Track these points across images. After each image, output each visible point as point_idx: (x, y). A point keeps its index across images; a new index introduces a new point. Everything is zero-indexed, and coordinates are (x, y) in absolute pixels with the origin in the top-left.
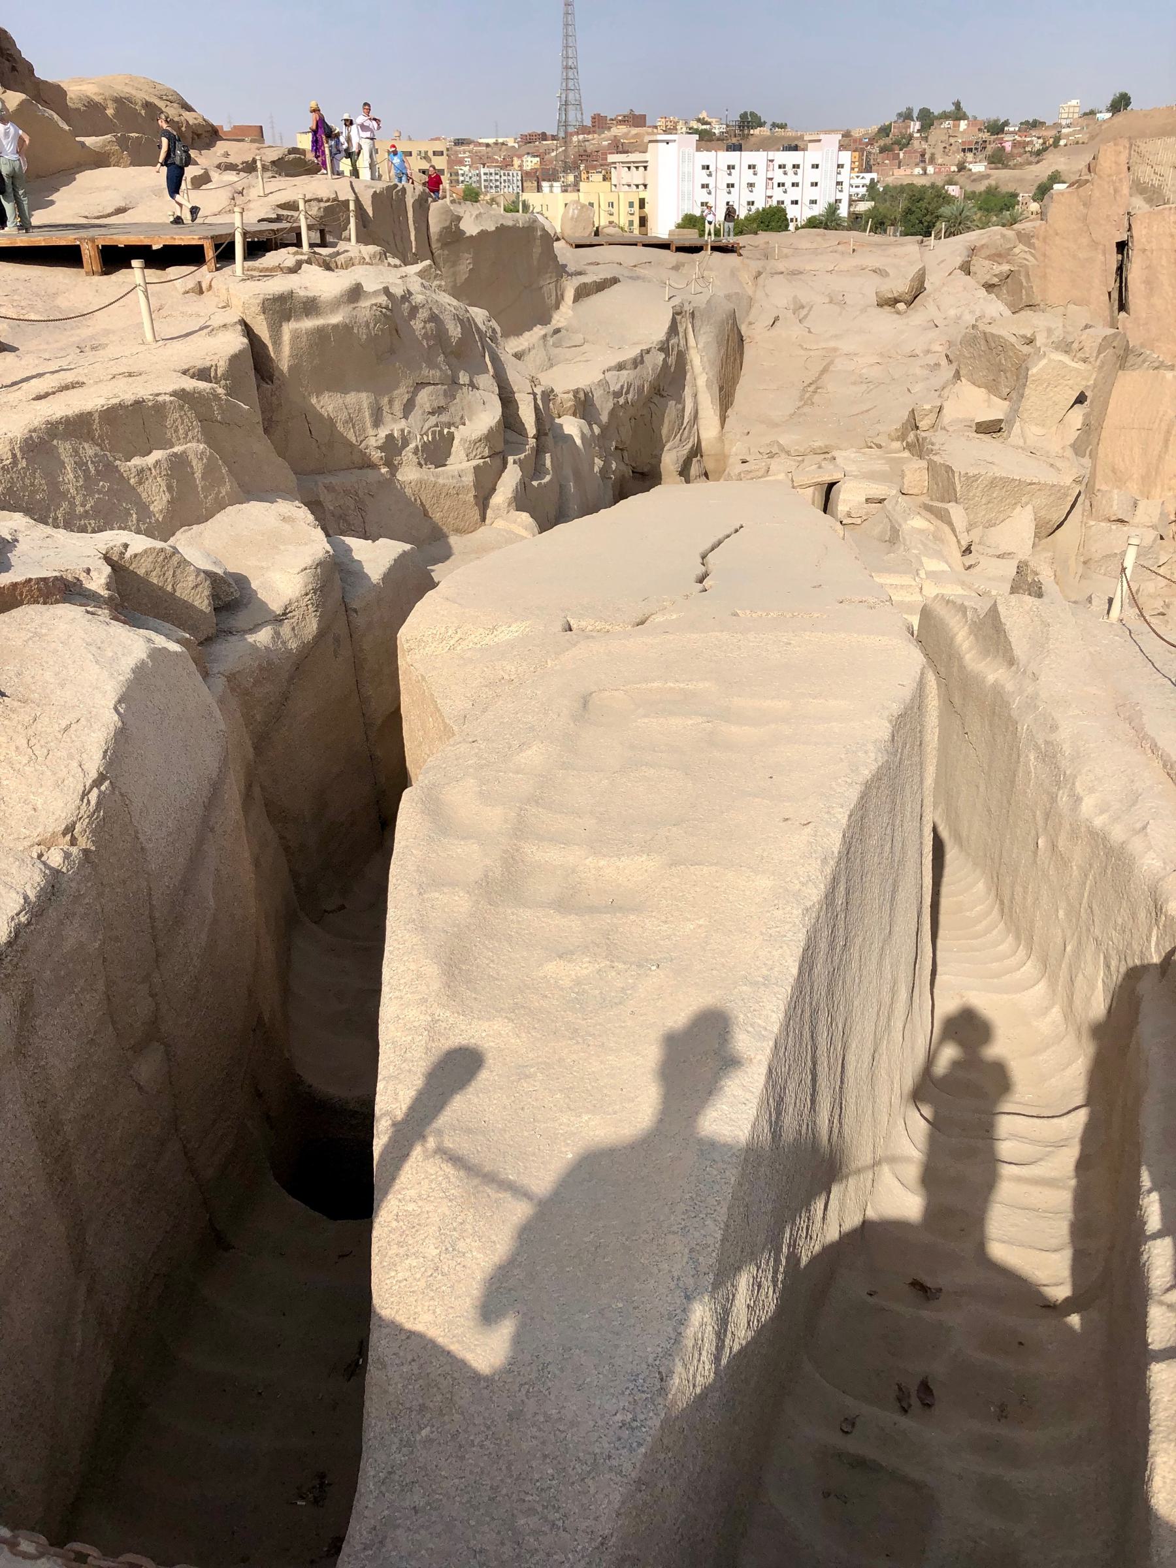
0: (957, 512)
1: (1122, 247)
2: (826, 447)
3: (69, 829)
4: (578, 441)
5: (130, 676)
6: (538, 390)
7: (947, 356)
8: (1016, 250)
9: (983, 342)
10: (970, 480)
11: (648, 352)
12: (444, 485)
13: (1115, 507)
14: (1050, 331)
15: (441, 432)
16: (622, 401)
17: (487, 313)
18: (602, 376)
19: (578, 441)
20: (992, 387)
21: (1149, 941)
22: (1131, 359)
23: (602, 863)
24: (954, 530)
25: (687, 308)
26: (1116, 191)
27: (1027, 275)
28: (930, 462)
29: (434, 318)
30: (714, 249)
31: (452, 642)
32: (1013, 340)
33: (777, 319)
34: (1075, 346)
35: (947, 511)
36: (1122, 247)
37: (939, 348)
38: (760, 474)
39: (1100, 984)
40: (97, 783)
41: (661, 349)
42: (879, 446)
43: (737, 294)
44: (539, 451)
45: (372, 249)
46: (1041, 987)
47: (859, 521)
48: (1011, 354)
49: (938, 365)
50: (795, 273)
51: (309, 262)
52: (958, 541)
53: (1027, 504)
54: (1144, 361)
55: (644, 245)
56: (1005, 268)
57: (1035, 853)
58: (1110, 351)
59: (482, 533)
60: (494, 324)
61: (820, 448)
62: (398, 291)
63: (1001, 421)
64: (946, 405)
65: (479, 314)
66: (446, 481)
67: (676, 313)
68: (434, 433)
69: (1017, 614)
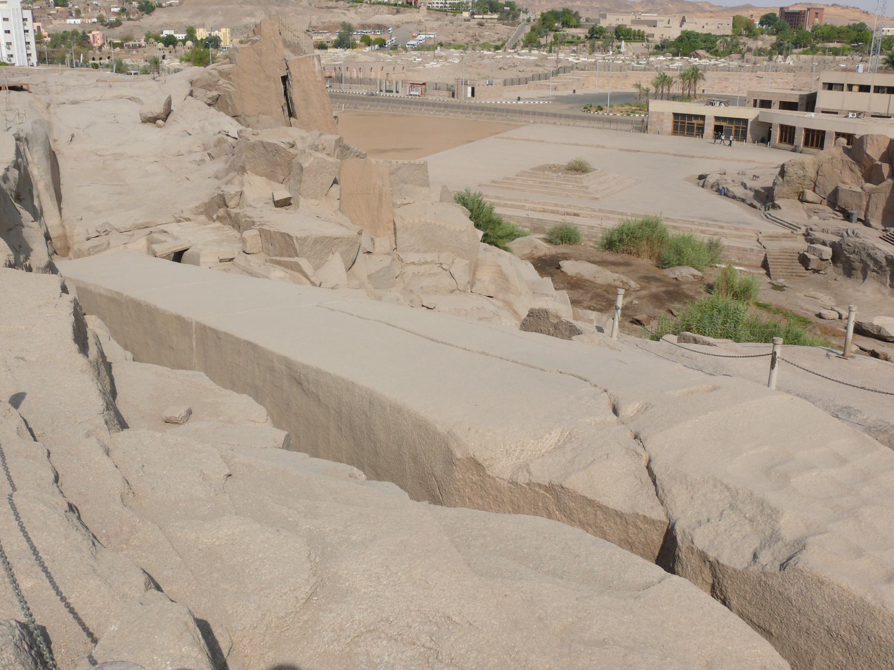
0: (303, 262)
1: (285, 79)
7: (209, 155)
8: (220, 82)
9: (261, 148)
11: (7, 169)
14: (303, 138)
24: (306, 276)
25: (22, 135)
26: (275, 46)
27: (230, 97)
32: (283, 145)
33: (73, 136)
34: (320, 147)
35: (297, 264)
36: (285, 79)
37: (197, 149)
38: (104, 247)
41: (14, 167)
42: (188, 220)
43: (40, 120)
48: (283, 154)
56: (215, 93)
61: (142, 224)
63: (290, 198)
64: (246, 189)
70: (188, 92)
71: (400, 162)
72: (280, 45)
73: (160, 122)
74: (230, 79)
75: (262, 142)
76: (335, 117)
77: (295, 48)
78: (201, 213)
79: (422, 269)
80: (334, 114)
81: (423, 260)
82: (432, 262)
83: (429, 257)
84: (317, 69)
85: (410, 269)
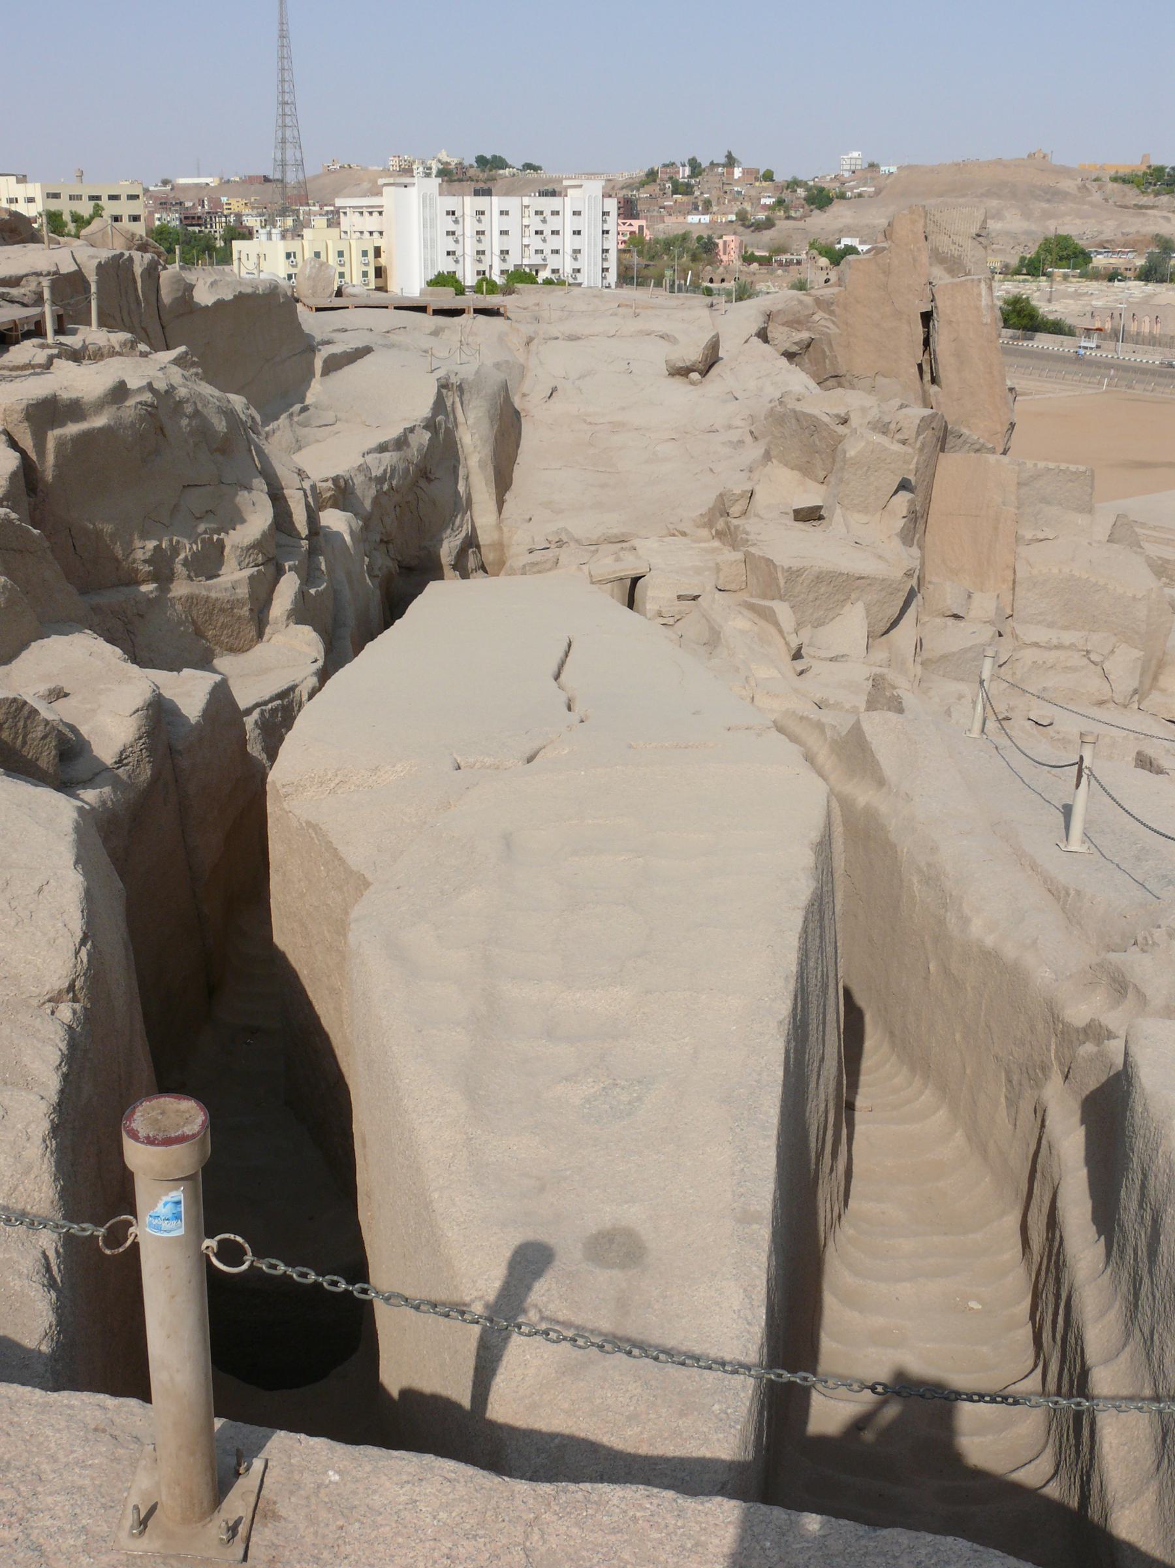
0: (782, 610)
2: (623, 534)
3: (71, 988)
4: (348, 538)
5: (74, 836)
6: (307, 485)
7: (752, 433)
8: (816, 317)
9: (793, 421)
10: (793, 574)
11: (412, 430)
12: (217, 599)
13: (949, 602)
14: (864, 410)
15: (211, 539)
16: (386, 487)
17: (244, 400)
18: (361, 461)
19: (348, 538)
20: (806, 470)
21: (1049, 1050)
22: (950, 441)
23: (578, 995)
24: (781, 632)
25: (454, 380)
26: (915, 260)
28: (747, 554)
29: (197, 413)
30: (478, 311)
31: (332, 785)
32: (826, 419)
34: (893, 426)
35: (771, 609)
36: (927, 317)
37: (740, 423)
38: (548, 566)
39: (1003, 1100)
40: (83, 942)
41: (426, 427)
42: (684, 534)
43: (507, 362)
44: (313, 552)
45: (120, 337)
46: (942, 1114)
47: (671, 621)
48: (825, 434)
49: (741, 442)
50: (573, 338)
51: (59, 356)
52: (787, 644)
53: (858, 599)
54: (965, 442)
55: (396, 308)
56: (805, 335)
57: (926, 979)
58: (930, 432)
59: (259, 649)
60: (252, 411)
62: (161, 386)
63: (820, 508)
64: (758, 489)
65: (237, 401)
66: (219, 595)
67: (444, 386)
68: (203, 541)
69: (879, 729)
70: (754, 330)
71: (1041, 465)
72: (924, 258)
73: (695, 376)
74: (832, 313)
75: (795, 412)
76: (1011, 389)
77: (953, 265)
78: (704, 526)
79: (1051, 656)
80: (1009, 383)
81: (1055, 642)
82: (1072, 647)
83: (1068, 637)
84: (984, 303)
85: (1029, 655)
